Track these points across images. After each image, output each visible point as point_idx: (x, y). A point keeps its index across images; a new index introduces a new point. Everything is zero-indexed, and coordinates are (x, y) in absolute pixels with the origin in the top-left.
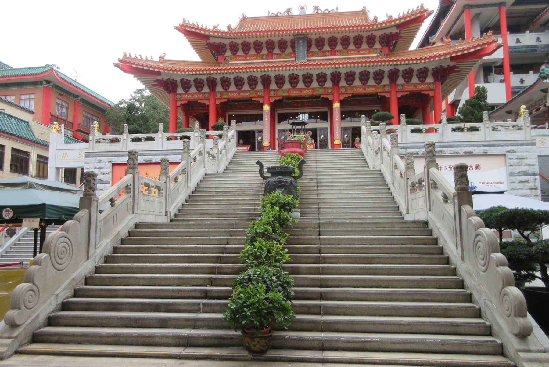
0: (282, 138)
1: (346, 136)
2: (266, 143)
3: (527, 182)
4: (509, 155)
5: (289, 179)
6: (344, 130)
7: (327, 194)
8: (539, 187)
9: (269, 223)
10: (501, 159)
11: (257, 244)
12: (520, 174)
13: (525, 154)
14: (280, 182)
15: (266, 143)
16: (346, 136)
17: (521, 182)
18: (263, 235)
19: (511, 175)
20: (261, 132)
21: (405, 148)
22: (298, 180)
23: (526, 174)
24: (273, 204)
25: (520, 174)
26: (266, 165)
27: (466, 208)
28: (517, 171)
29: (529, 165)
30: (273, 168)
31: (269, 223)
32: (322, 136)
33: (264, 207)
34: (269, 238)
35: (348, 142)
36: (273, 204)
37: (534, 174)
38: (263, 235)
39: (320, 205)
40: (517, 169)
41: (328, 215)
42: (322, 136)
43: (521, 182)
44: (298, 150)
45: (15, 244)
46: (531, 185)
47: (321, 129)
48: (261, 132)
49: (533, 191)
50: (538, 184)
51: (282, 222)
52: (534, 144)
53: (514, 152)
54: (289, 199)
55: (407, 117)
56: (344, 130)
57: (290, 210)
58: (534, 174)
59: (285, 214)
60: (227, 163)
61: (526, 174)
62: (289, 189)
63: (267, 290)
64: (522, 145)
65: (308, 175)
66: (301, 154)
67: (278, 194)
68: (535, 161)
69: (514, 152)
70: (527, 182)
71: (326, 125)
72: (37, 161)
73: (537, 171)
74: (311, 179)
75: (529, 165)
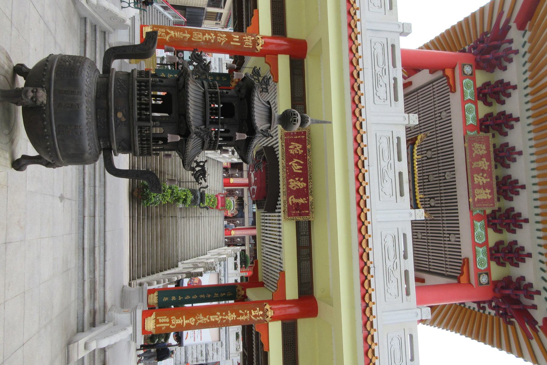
0: (237, 192)
1: (239, 239)
2: (232, 181)
3: (202, 355)
4: (219, 343)
5: (199, 201)
6: (243, 238)
7: (192, 222)
8: (198, 363)
9: (177, 194)
10: (217, 339)
11: (169, 190)
12: (207, 350)
13: (220, 353)
14: (197, 197)
15: (232, 181)
16: (239, 239)
17: (202, 352)
18: (173, 192)
19: (206, 345)
20: (242, 176)
21: (224, 276)
22: (198, 206)
23: (207, 354)
24: (186, 195)
25: (207, 350)
26: (206, 190)
27: (184, 275)
28: (209, 349)
29: (213, 356)
30: (204, 194)
31: (177, 194)
32: (238, 222)
33: (184, 191)
34: (171, 195)
35: (234, 242)
36: (186, 195)
37: (206, 360)
38: (173, 192)
39: (185, 219)
40: (210, 349)
41: (181, 222)
42: (238, 222)
43: (202, 352)
44: (220, 205)
45: (157, 10)
46: (200, 358)
47: (244, 221)
48: (242, 176)
49: (196, 360)
50: (200, 362)
51: (178, 200)
52: (227, 359)
53: (222, 346)
54: (189, 202)
55: (247, 278)
56: (243, 238)
57: (183, 203)
58: (206, 360)
59: (181, 201)
60: (214, 158)
61: (207, 354)
62: (194, 202)
63: (154, 197)
64: (226, 351)
65: (204, 212)
66: (217, 207)
67: (191, 197)
68: (215, 360)
69: (222, 346)
70: (202, 355)
71: (247, 225)
72: (218, 13)
73: (209, 361)
74: (201, 214)
75: (213, 356)
